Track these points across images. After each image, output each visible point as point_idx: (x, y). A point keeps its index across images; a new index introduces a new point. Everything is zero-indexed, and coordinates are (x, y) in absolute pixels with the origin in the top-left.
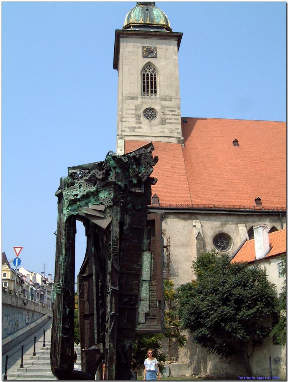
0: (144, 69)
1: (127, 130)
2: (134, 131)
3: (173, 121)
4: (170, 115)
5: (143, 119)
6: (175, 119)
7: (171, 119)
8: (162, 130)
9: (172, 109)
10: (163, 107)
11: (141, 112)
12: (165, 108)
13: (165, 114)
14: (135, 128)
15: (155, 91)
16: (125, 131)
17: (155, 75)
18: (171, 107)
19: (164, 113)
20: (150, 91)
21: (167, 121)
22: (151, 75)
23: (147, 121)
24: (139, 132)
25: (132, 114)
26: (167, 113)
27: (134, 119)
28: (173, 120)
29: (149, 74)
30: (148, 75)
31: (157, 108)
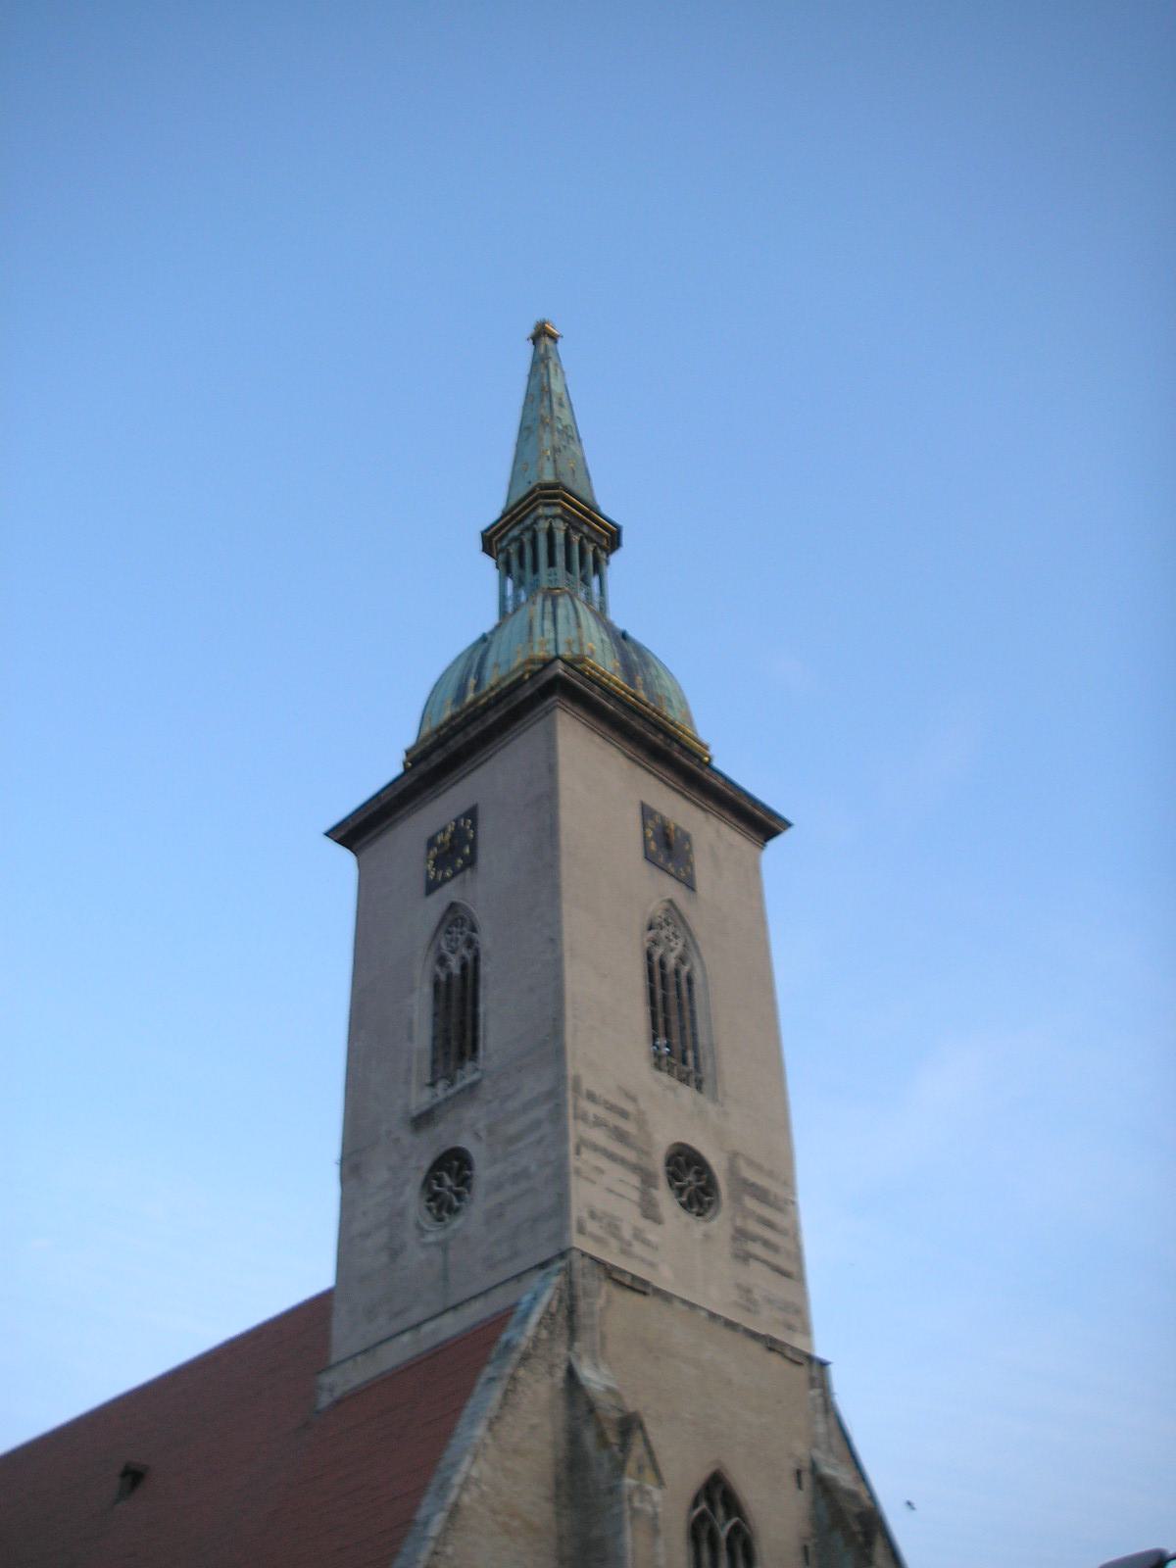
17: (476, 959)
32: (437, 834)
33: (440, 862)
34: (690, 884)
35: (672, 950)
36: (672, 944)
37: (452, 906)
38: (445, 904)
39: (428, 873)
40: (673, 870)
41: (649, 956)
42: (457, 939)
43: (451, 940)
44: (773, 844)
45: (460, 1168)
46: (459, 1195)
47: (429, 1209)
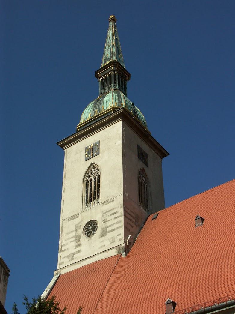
0: (87, 174)
1: (66, 260)
2: (73, 259)
3: (115, 226)
5: (84, 239)
6: (117, 223)
7: (113, 225)
8: (102, 244)
9: (114, 211)
10: (105, 213)
11: (80, 231)
12: (107, 213)
13: (106, 221)
14: (74, 254)
15: (98, 197)
16: (63, 263)
17: (99, 177)
18: (113, 209)
20: (92, 198)
21: (109, 229)
22: (95, 178)
23: (87, 239)
24: (78, 257)
25: (72, 238)
26: (108, 218)
28: (115, 224)
29: (92, 177)
30: (91, 180)
31: (98, 218)
32: (89, 146)
33: (89, 153)
34: (147, 165)
35: (143, 180)
36: (143, 179)
37: (92, 163)
38: (90, 163)
39: (86, 155)
40: (144, 162)
41: (139, 181)
42: (93, 172)
43: (91, 172)
44: (165, 159)
45: (94, 224)
46: (93, 230)
47: (85, 234)
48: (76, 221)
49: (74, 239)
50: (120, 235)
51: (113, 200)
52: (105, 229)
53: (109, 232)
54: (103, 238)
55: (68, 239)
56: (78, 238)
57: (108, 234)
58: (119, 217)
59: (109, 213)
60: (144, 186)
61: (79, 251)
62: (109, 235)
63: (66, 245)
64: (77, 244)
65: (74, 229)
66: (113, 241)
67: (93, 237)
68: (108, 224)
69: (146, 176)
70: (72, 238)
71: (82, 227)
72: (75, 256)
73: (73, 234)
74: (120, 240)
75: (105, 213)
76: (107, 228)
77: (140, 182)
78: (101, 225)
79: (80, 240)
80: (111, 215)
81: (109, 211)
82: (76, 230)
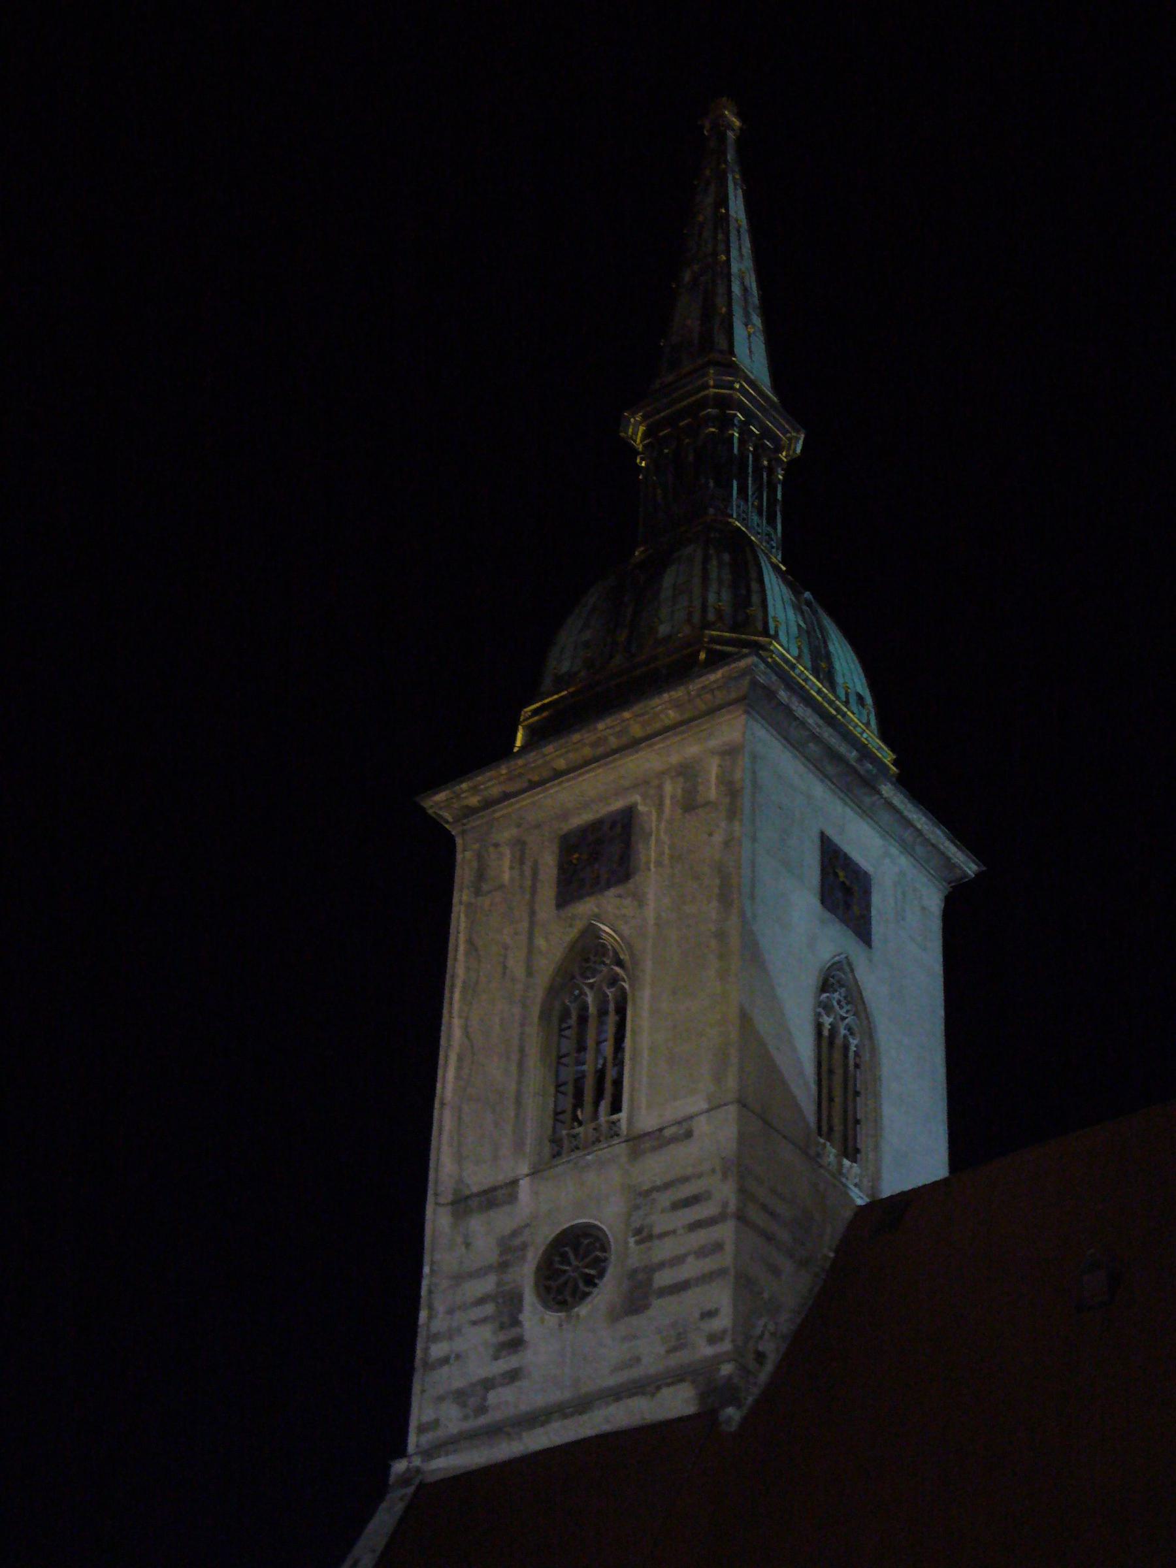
2: (482, 1409)
3: (691, 1269)
4: (674, 1232)
6: (702, 1253)
7: (677, 1261)
10: (642, 1196)
11: (525, 1274)
12: (655, 1195)
13: (650, 1237)
14: (488, 1384)
18: (685, 1179)
19: (645, 1234)
21: (663, 1278)
23: (552, 1318)
24: (506, 1401)
25: (481, 1301)
26: (662, 1222)
27: (486, 1333)
28: (691, 1259)
31: (609, 1216)
41: (819, 1027)
48: (503, 1221)
49: (489, 1309)
50: (709, 1314)
51: (689, 1134)
52: (641, 1276)
53: (664, 1292)
54: (634, 1320)
55: (464, 1307)
56: (508, 1307)
57: (657, 1303)
58: (711, 1222)
59: (665, 1199)
60: (846, 1047)
61: (513, 1376)
62: (663, 1311)
63: (450, 1335)
64: (503, 1337)
65: (493, 1258)
66: (679, 1343)
67: (583, 1310)
68: (663, 1250)
69: (855, 999)
70: (481, 1301)
71: (533, 1258)
72: (493, 1397)
73: (488, 1285)
74: (713, 1339)
75: (648, 1193)
76: (652, 1269)
77: (826, 1033)
78: (625, 1255)
79: (521, 1317)
80: (676, 1206)
81: (667, 1186)
82: (503, 1266)
